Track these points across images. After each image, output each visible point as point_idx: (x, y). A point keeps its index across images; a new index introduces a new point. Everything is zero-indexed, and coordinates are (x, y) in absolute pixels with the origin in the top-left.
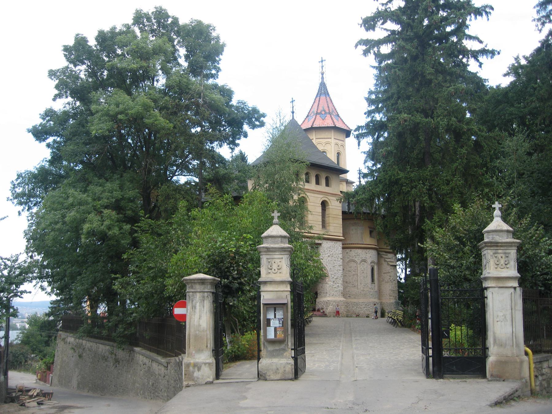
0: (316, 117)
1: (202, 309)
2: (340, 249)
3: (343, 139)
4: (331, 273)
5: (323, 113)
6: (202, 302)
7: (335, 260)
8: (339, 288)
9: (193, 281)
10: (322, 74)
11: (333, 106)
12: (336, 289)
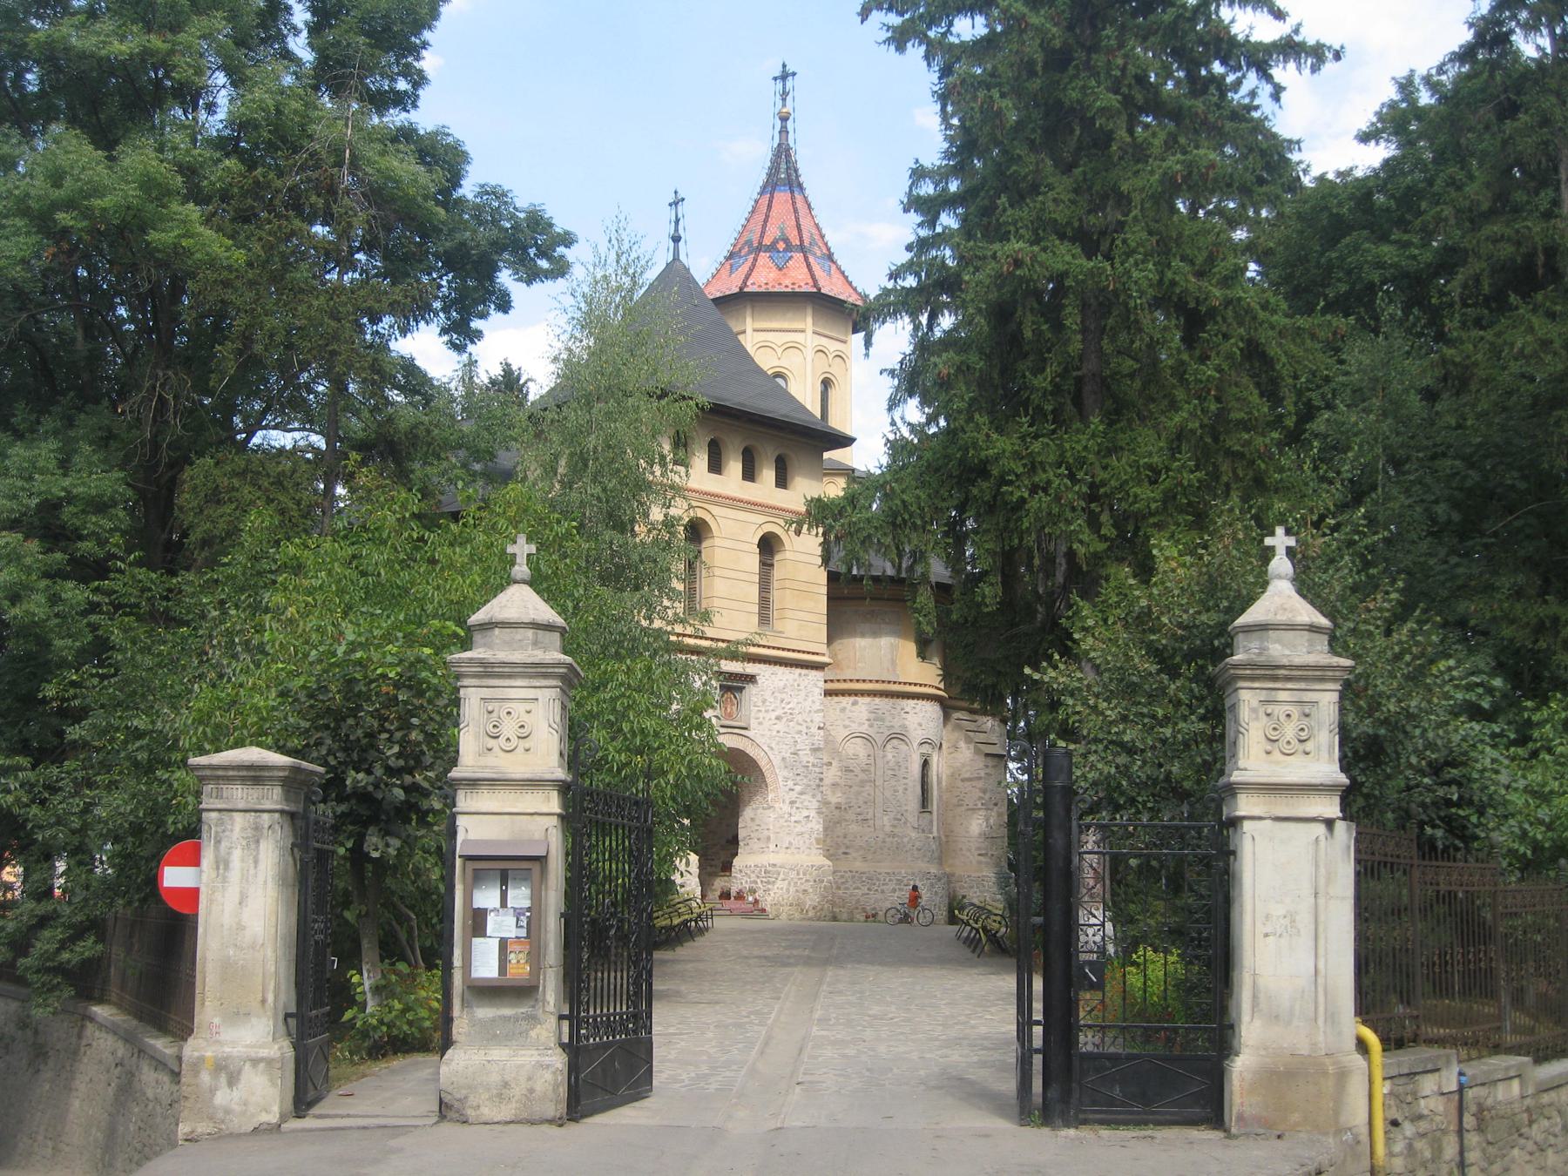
0: (755, 260)
1: (252, 871)
2: (817, 692)
3: (843, 338)
5: (781, 246)
6: (253, 846)
7: (800, 732)
8: (810, 825)
9: (220, 773)
10: (784, 119)
11: (817, 225)
12: (799, 828)
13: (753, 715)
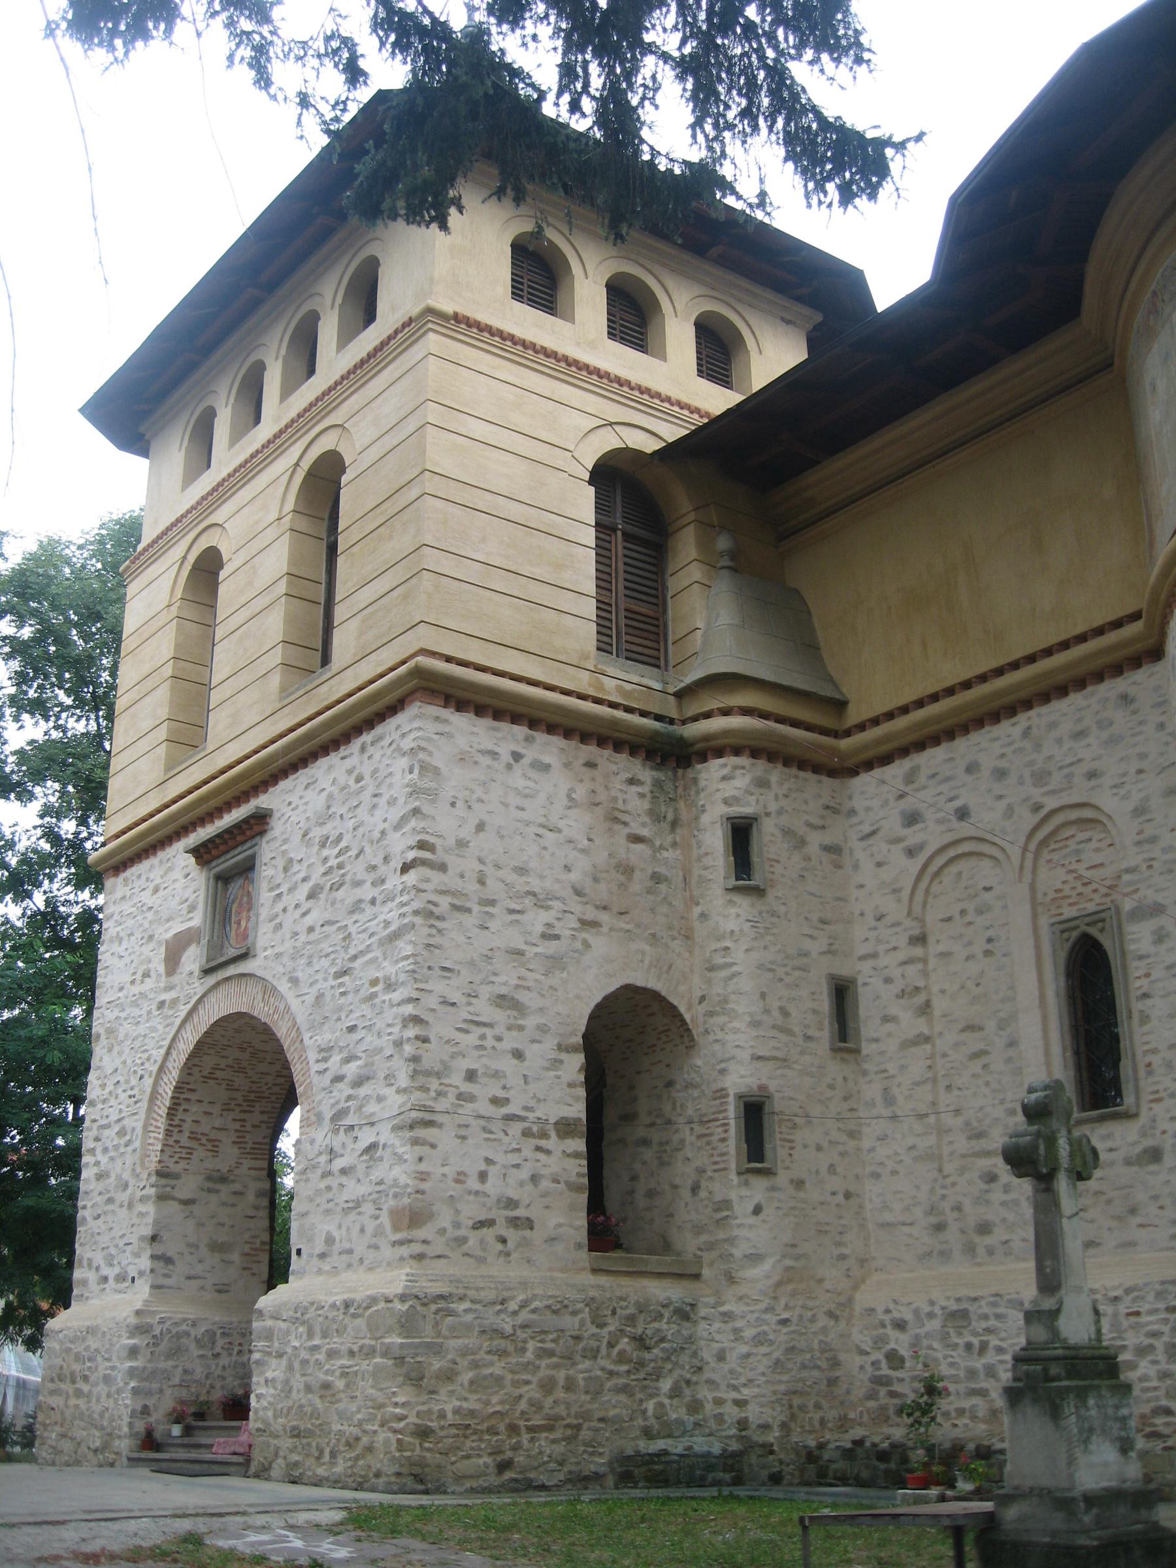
4: (325, 1037)
13: (264, 913)
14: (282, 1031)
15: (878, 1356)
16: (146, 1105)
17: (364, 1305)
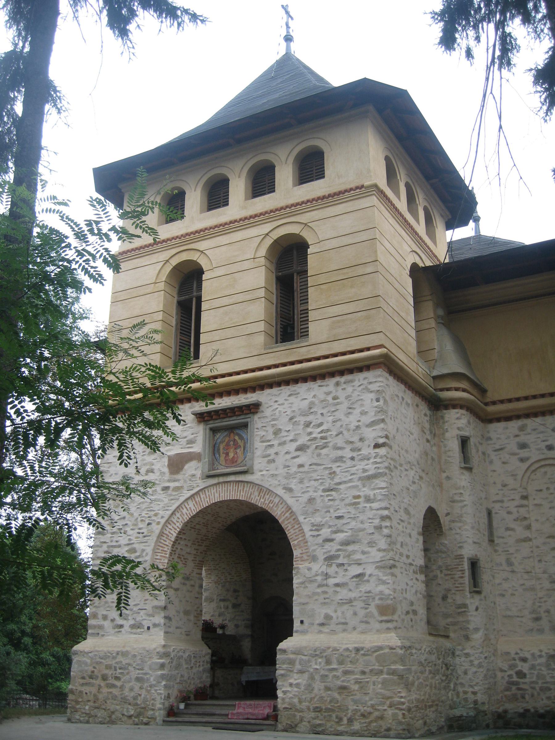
4: (317, 519)
7: (340, 459)
8: (364, 588)
12: (344, 594)
13: (258, 453)
14: (277, 513)
15: (512, 672)
16: (155, 539)
17: (373, 650)
